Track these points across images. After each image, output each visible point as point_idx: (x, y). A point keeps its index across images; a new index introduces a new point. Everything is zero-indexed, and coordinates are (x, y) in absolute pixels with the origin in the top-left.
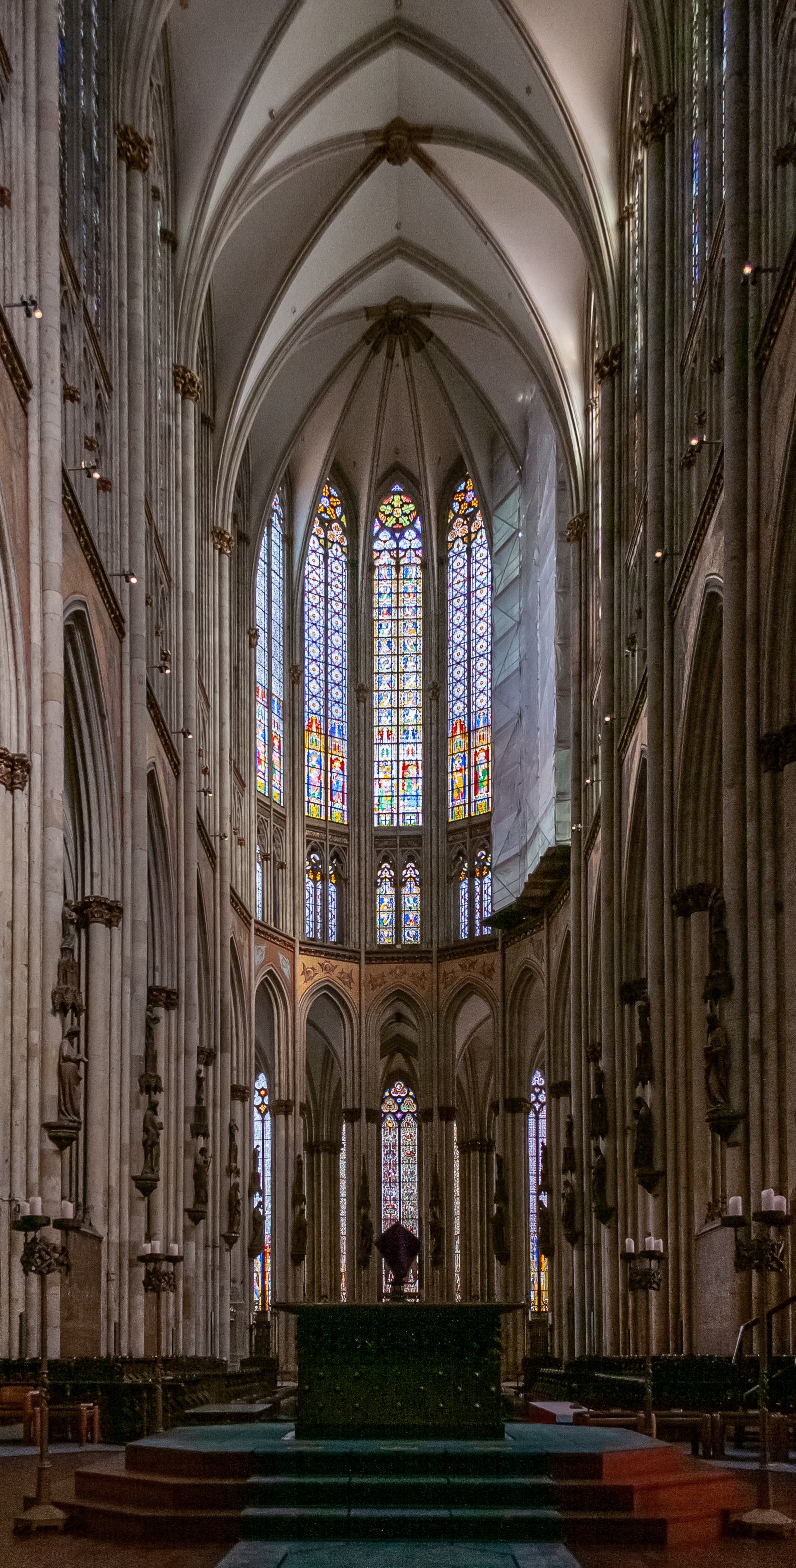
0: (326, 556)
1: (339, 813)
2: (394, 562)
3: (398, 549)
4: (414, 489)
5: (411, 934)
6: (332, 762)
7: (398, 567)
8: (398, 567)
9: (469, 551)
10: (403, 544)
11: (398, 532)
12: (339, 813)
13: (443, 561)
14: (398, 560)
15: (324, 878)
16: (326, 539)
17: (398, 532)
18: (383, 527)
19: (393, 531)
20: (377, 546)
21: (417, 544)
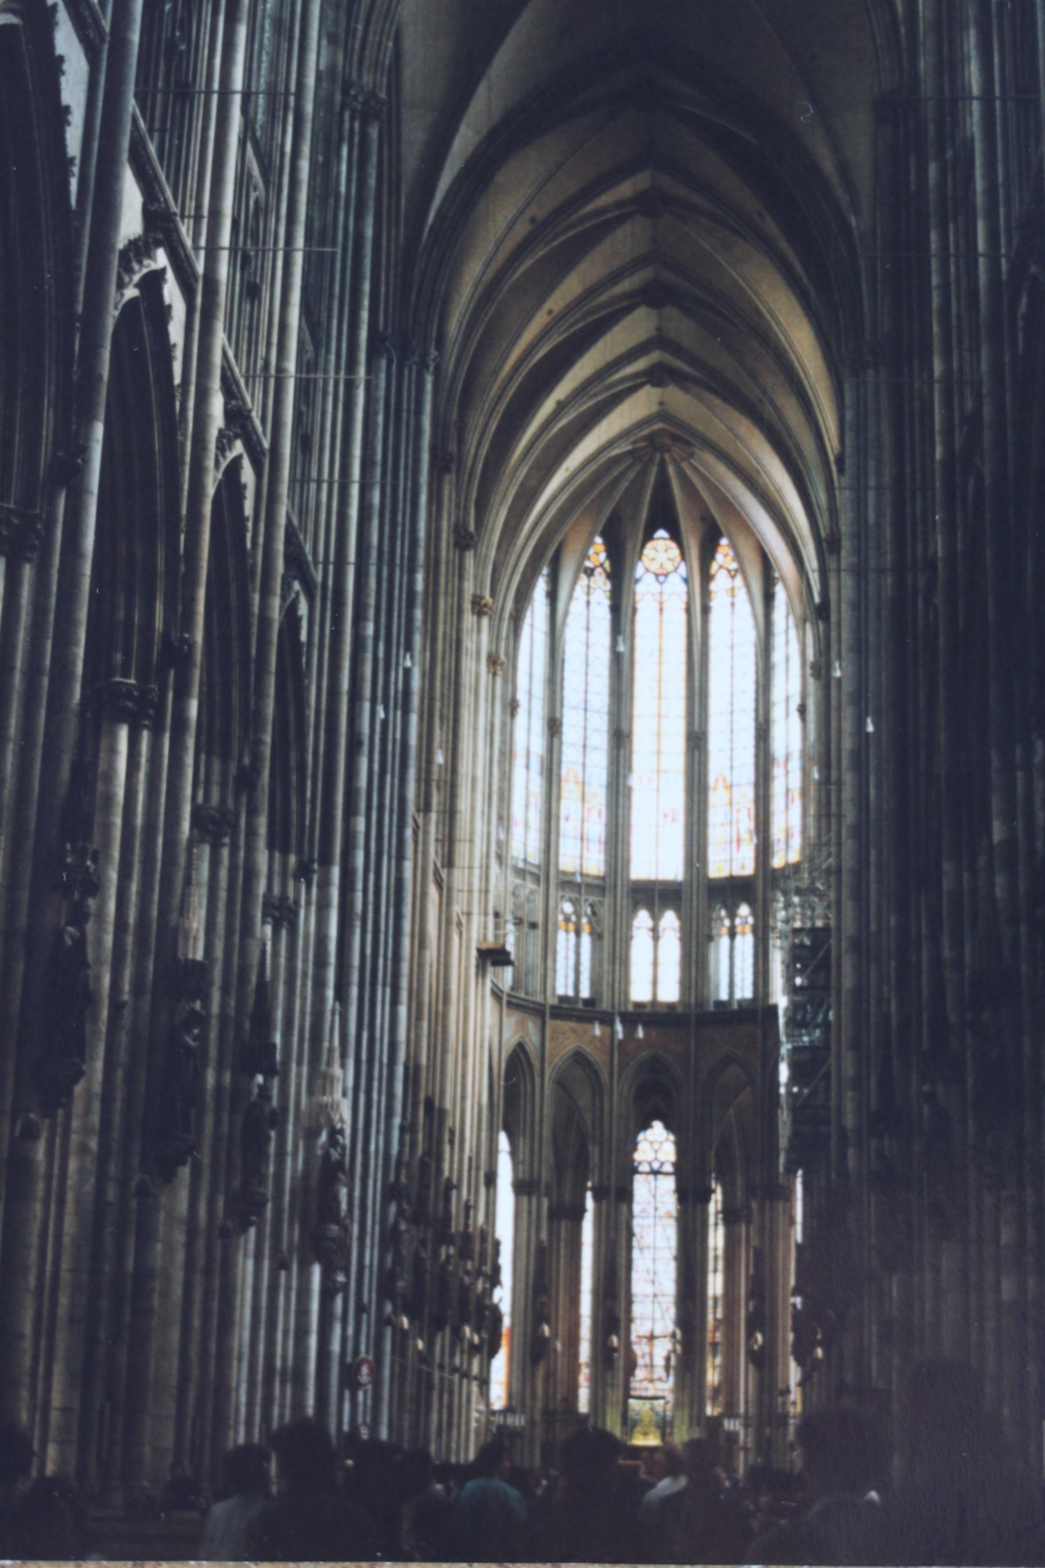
0: (588, 603)
1: (595, 864)
2: (657, 606)
3: (661, 593)
4: (676, 536)
5: (670, 992)
6: (589, 810)
7: (661, 610)
8: (661, 610)
9: (733, 605)
10: (667, 588)
11: (661, 576)
12: (595, 864)
13: (706, 610)
14: (661, 603)
15: (578, 933)
16: (589, 587)
17: (661, 576)
18: (647, 570)
19: (657, 575)
20: (640, 589)
21: (683, 588)
